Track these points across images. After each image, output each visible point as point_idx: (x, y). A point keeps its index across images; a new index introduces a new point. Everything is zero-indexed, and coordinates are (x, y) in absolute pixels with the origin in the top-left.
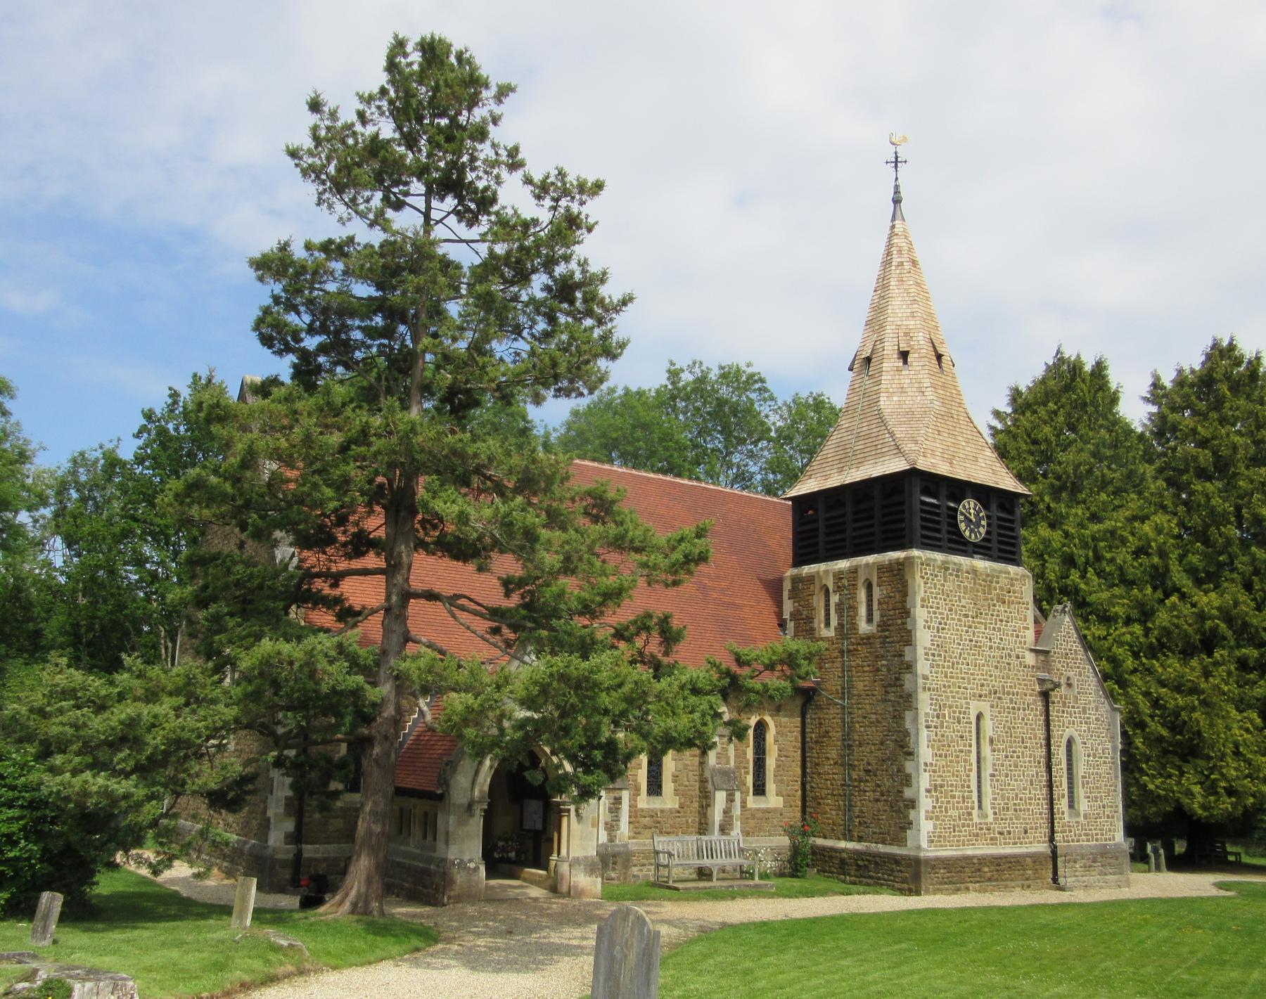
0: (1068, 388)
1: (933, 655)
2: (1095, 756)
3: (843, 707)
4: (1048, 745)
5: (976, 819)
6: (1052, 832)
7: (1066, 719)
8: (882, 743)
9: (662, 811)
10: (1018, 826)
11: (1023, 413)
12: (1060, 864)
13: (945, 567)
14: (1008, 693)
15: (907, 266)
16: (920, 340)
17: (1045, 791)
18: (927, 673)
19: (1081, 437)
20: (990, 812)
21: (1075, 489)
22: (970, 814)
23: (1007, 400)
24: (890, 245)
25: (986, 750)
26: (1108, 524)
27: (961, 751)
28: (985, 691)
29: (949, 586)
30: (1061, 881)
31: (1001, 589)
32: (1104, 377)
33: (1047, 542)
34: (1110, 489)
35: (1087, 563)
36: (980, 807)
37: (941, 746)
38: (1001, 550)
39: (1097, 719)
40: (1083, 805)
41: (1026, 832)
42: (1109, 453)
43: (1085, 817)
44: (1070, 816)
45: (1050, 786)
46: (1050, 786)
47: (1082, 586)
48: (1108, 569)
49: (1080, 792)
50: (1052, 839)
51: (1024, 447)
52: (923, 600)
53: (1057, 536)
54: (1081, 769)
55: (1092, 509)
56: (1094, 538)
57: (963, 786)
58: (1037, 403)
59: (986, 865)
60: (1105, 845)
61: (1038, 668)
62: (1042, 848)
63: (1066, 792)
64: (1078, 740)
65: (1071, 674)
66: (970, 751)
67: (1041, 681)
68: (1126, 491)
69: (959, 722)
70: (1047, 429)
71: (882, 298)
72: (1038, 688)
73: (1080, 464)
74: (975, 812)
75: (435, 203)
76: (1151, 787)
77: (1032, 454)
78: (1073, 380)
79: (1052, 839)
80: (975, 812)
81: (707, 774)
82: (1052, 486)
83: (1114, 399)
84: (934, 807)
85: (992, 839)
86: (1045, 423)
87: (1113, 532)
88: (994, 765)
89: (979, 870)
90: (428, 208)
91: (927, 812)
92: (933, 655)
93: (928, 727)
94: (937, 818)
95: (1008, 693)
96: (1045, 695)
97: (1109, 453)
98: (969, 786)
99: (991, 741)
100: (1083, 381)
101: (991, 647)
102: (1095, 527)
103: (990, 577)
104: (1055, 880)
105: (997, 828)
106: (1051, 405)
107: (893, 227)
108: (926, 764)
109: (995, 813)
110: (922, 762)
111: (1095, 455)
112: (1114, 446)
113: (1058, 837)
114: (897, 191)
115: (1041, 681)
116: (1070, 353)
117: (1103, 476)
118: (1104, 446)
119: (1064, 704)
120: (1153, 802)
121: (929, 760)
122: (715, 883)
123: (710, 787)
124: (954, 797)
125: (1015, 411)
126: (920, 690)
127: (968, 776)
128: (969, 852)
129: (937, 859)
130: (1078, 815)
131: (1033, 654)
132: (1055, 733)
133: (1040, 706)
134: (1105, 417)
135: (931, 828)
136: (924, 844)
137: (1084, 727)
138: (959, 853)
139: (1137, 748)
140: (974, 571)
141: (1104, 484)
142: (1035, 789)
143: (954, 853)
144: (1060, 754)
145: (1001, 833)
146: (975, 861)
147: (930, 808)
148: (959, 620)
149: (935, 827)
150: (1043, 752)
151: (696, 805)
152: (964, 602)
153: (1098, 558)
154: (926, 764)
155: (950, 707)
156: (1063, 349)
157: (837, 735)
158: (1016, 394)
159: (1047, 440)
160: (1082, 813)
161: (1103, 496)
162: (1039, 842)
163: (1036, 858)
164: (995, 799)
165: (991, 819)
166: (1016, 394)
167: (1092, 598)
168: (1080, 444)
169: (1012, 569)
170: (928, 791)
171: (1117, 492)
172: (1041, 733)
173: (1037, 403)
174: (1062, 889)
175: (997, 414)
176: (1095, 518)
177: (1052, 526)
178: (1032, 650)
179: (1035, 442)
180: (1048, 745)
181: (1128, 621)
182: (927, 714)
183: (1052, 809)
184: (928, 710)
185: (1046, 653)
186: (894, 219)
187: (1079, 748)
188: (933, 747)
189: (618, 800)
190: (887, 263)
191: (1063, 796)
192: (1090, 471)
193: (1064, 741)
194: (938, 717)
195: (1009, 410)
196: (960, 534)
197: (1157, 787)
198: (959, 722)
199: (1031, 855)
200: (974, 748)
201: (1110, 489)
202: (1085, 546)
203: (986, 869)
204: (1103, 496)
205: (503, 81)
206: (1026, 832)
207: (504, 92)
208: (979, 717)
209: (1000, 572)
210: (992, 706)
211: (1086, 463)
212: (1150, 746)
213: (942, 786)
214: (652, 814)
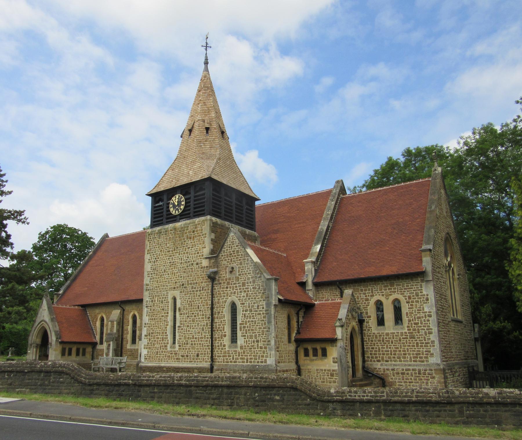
1: (152, 274)
2: (251, 311)
5: (169, 349)
9: (134, 349)
10: (193, 353)
13: (160, 232)
14: (191, 284)
18: (148, 283)
22: (166, 346)
27: (163, 316)
28: (178, 285)
29: (161, 240)
31: (190, 232)
37: (152, 316)
38: (195, 212)
40: (241, 341)
41: (198, 355)
43: (241, 347)
44: (230, 347)
49: (239, 333)
52: (148, 251)
57: (163, 333)
60: (256, 366)
61: (210, 267)
65: (234, 265)
66: (167, 316)
69: (162, 302)
84: (148, 343)
85: (177, 359)
88: (181, 321)
91: (145, 345)
92: (152, 274)
93: (147, 307)
94: (150, 348)
95: (191, 284)
98: (166, 333)
99: (179, 310)
101: (181, 263)
103: (182, 229)
105: (181, 353)
108: (145, 324)
109: (180, 346)
110: (144, 323)
114: (206, 59)
119: (228, 283)
121: (147, 322)
124: (158, 338)
126: (145, 291)
127: (166, 328)
128: (162, 365)
129: (146, 367)
130: (236, 347)
131: (208, 260)
135: (146, 353)
136: (143, 360)
138: (158, 365)
140: (175, 229)
142: (205, 333)
143: (155, 365)
145: (182, 356)
146: (165, 369)
147: (146, 344)
148: (165, 254)
149: (148, 352)
150: (209, 313)
152: (168, 245)
154: (145, 324)
155: (158, 296)
162: (206, 362)
164: (180, 339)
169: (197, 220)
170: (146, 336)
172: (210, 302)
178: (206, 258)
182: (147, 301)
184: (148, 299)
188: (149, 315)
189: (109, 345)
191: (225, 336)
194: (152, 301)
196: (172, 214)
198: (162, 302)
199: (196, 368)
206: (198, 355)
208: (175, 299)
209: (190, 224)
210: (181, 292)
213: (152, 333)
214: (131, 350)
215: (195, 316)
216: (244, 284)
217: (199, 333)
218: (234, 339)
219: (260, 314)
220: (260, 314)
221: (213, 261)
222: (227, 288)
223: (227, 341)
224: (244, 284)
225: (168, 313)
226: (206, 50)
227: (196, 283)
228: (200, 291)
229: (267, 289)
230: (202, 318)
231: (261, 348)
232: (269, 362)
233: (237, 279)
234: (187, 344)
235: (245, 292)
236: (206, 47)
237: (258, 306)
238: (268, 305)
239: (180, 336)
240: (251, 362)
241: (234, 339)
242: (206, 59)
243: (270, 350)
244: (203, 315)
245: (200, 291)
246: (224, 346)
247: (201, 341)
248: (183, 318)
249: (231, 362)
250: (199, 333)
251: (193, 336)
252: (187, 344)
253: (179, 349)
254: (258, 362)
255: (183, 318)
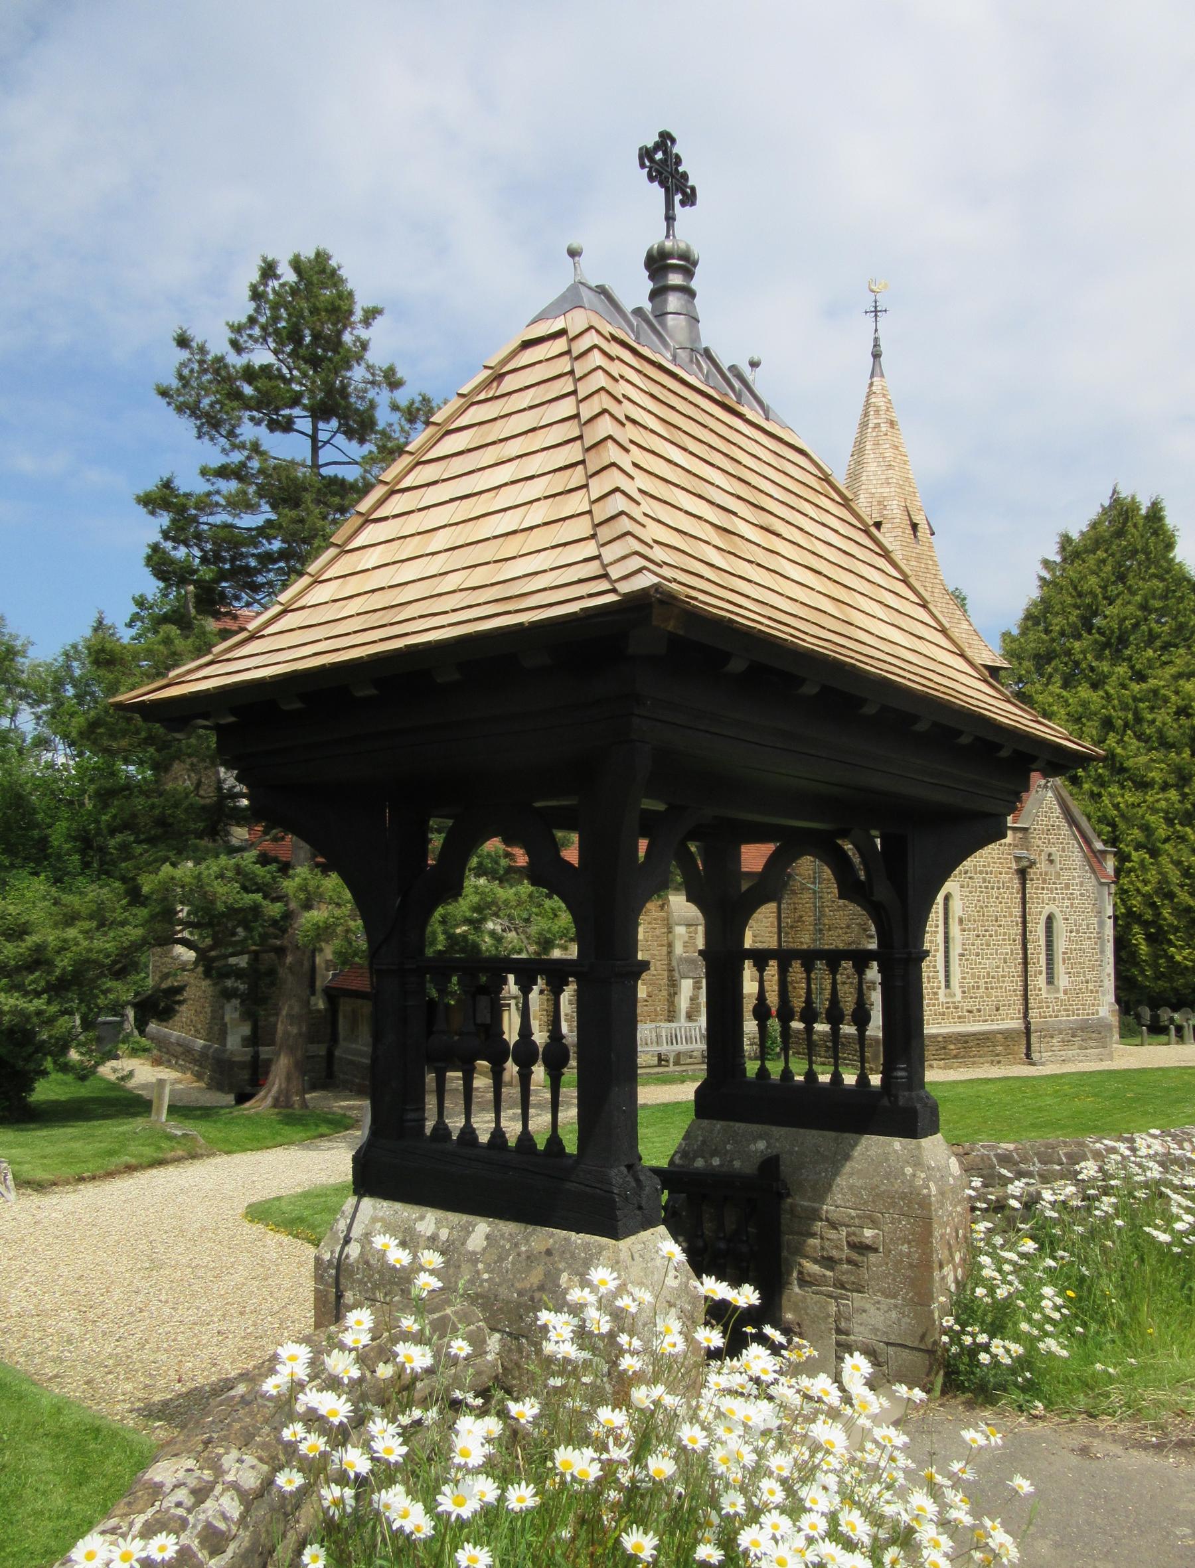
0: (1120, 533)
2: (1078, 931)
3: (815, 892)
4: (1024, 923)
6: (1026, 1009)
7: (1046, 895)
8: (848, 927)
10: (991, 1003)
11: (1072, 562)
12: (1033, 1039)
14: (981, 872)
15: (884, 427)
16: (895, 509)
17: (1020, 968)
19: (1129, 589)
20: (958, 992)
21: (1123, 641)
22: (936, 994)
23: (1056, 548)
24: (867, 405)
25: (955, 930)
26: (1152, 683)
30: (1035, 1056)
32: (1161, 519)
33: (1084, 704)
34: (1158, 643)
35: (1126, 725)
36: (947, 986)
39: (1082, 895)
40: (1063, 981)
41: (998, 1009)
42: (1158, 604)
43: (1065, 993)
44: (1048, 992)
45: (1025, 962)
46: (1025, 962)
47: (1119, 750)
48: (1148, 731)
49: (1060, 968)
50: (1026, 1015)
51: (1069, 600)
53: (1095, 697)
54: (1060, 945)
55: (1138, 667)
56: (1135, 699)
58: (1087, 551)
59: (952, 1043)
61: (1016, 846)
62: (1017, 1024)
63: (1044, 969)
64: (1059, 917)
66: (936, 932)
67: (1018, 859)
68: (1176, 646)
70: (1093, 580)
71: (858, 463)
72: (1014, 866)
73: (1125, 618)
74: (942, 992)
75: (321, 425)
76: (1178, 958)
77: (1078, 608)
78: (1125, 524)
79: (1026, 1015)
80: (942, 992)
81: (674, 964)
82: (1096, 642)
83: (1170, 546)
85: (959, 1017)
86: (1093, 573)
87: (1155, 692)
89: (944, 1048)
90: (315, 429)
95: (981, 872)
96: (1022, 873)
97: (1158, 604)
98: (935, 967)
99: (961, 921)
100: (1135, 526)
102: (1136, 687)
104: (1028, 1056)
106: (1101, 554)
107: (871, 385)
109: (964, 992)
111: (1144, 607)
112: (1165, 597)
113: (1032, 1013)
115: (1018, 859)
116: (1125, 493)
117: (1150, 630)
118: (1154, 597)
119: (1044, 881)
120: (1182, 974)
122: (671, 1068)
123: (676, 975)
125: (1064, 560)
130: (1057, 991)
132: (1032, 909)
133: (1016, 884)
134: (1158, 566)
137: (1067, 903)
139: (1165, 919)
141: (1152, 638)
142: (1009, 967)
144: (1038, 932)
146: (940, 1039)
151: (665, 993)
153: (1139, 719)
156: (1119, 488)
157: (809, 919)
158: (1066, 540)
159: (1091, 592)
160: (1062, 989)
161: (1150, 652)
162: (1012, 1019)
163: (1007, 1035)
164: (964, 978)
165: (959, 997)
166: (1066, 540)
167: (1129, 764)
168: (1127, 597)
171: (1165, 647)
172: (1017, 911)
173: (1087, 551)
174: (1034, 1064)
175: (1046, 563)
176: (1141, 677)
177: (1095, 686)
179: (1080, 595)
180: (1024, 923)
181: (1165, 787)
183: (1026, 986)
185: (1026, 829)
186: (872, 376)
187: (1060, 925)
190: (864, 425)
192: (1136, 626)
193: (1043, 918)
195: (1058, 559)
197: (1185, 958)
199: (1001, 1032)
200: (941, 929)
201: (1158, 643)
202: (1125, 707)
203: (952, 1047)
204: (1150, 652)
205: (370, 304)
206: (998, 1009)
207: (371, 314)
210: (962, 887)
211: (1132, 616)
212: (1178, 917)
215: (991, 936)
216: (1067, 886)
217: (998, 967)
218: (1050, 980)
219: (1089, 938)
220: (1089, 938)
221: (1019, 835)
222: (1043, 889)
223: (1042, 979)
224: (1067, 886)
225: (937, 926)
226: (876, 316)
227: (991, 873)
228: (999, 888)
229: (1099, 899)
230: (1004, 940)
231: (1092, 992)
232: (1101, 1014)
233: (1058, 876)
234: (978, 987)
235: (1069, 899)
236: (876, 311)
237: (1088, 925)
238: (1101, 924)
239: (963, 972)
240: (1078, 1015)
241: (1050, 980)
242: (876, 344)
243: (1103, 994)
244: (1005, 934)
245: (999, 888)
246: (1040, 990)
247: (1003, 982)
248: (968, 939)
249: (1051, 1016)
250: (998, 967)
251: (988, 973)
252: (978, 987)
253: (963, 998)
254: (1088, 1014)
255: (968, 939)
